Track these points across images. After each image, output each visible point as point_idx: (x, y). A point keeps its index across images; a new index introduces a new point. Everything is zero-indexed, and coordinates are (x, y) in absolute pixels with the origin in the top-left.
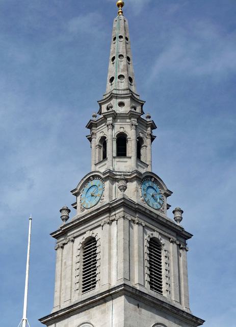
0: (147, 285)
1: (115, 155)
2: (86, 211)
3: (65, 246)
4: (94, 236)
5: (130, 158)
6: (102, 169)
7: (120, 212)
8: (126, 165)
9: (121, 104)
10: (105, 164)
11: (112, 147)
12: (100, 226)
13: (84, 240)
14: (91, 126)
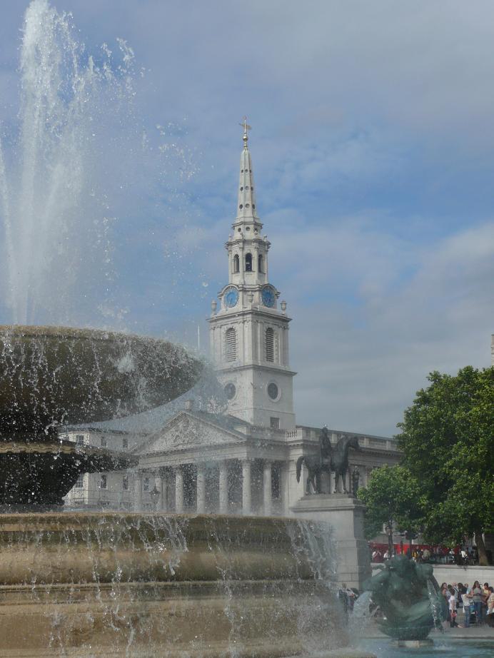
7: (249, 317)
8: (252, 279)
9: (248, 229)
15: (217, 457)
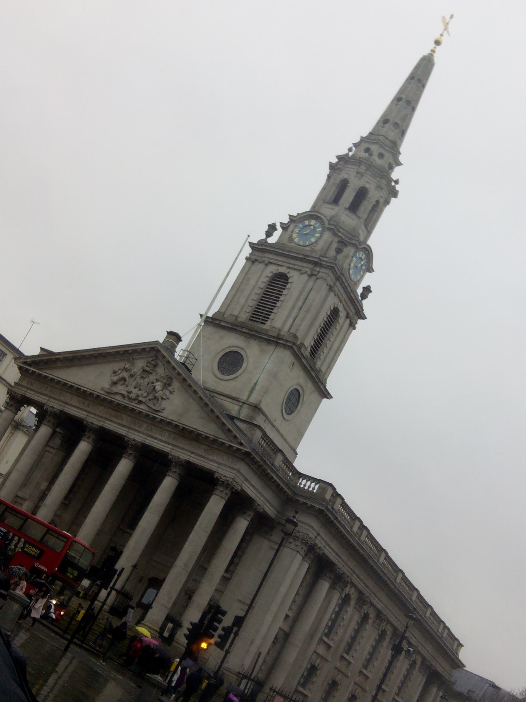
0: (309, 349)
1: (347, 207)
2: (293, 245)
3: (256, 263)
4: (289, 276)
5: (359, 217)
6: (328, 211)
9: (381, 156)
10: (333, 209)
11: (348, 196)
12: (300, 270)
13: (277, 272)
14: (341, 158)
15: (182, 452)
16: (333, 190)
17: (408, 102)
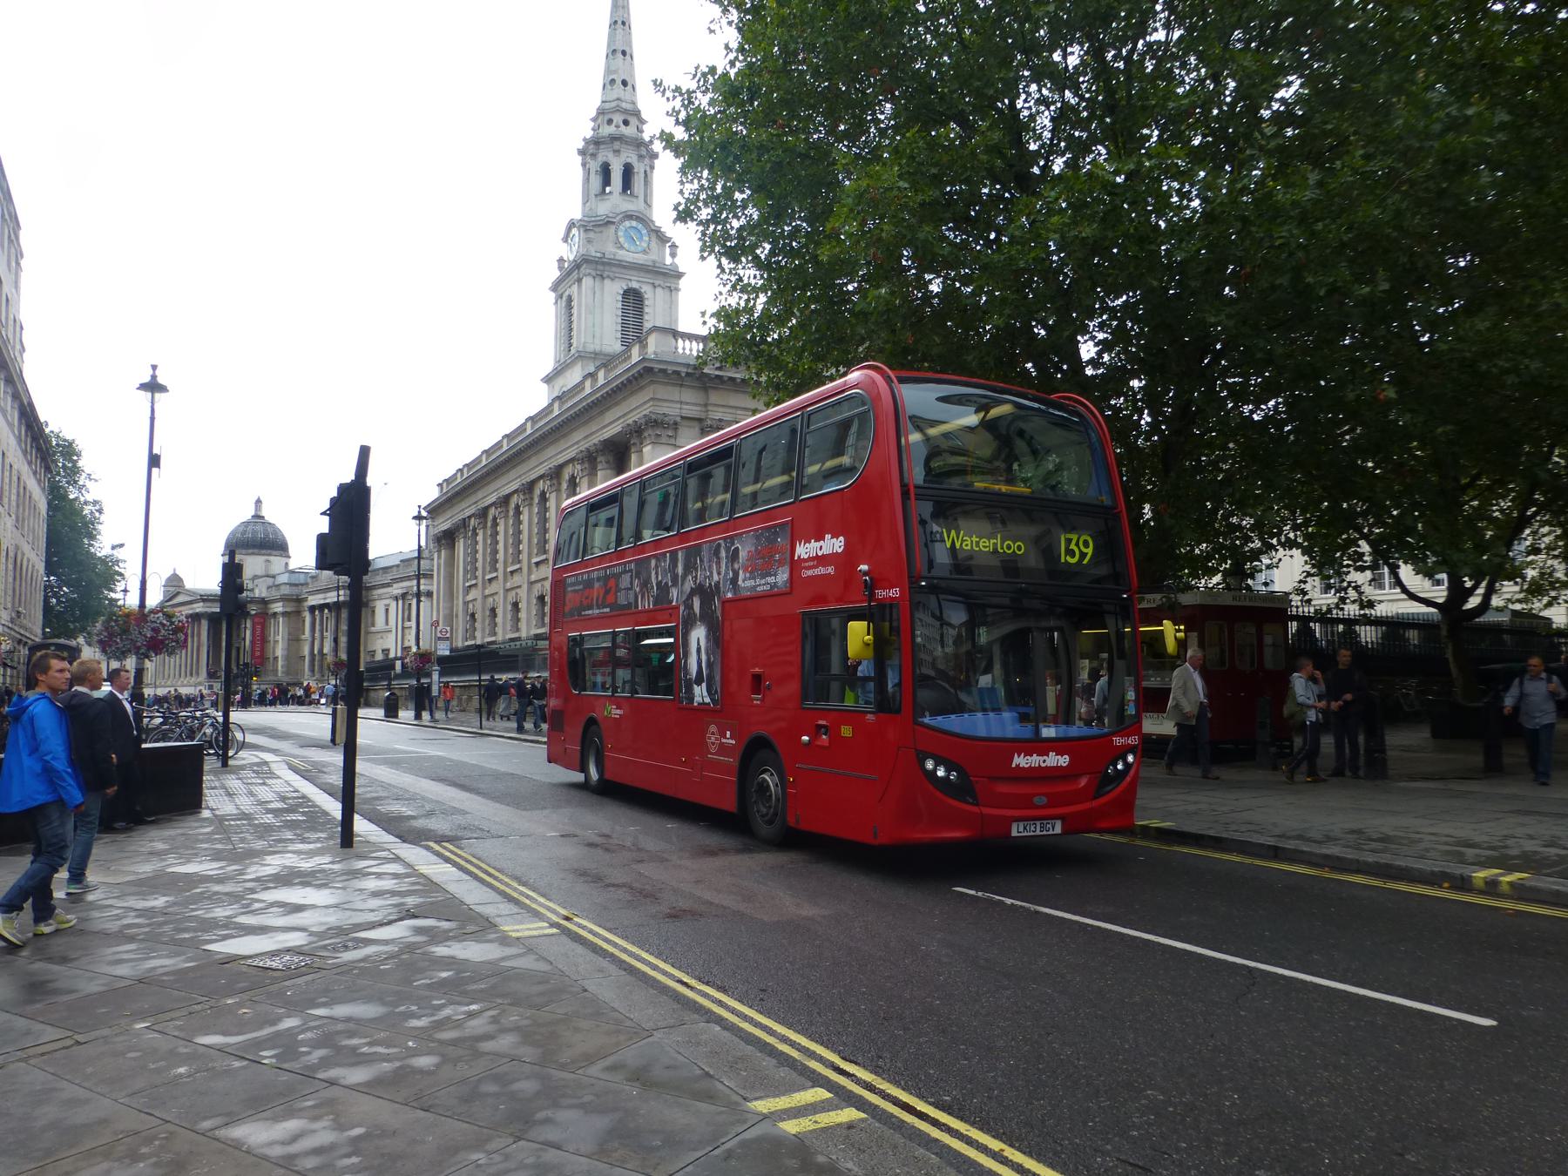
9: (626, 123)
16: (596, 181)
17: (624, 53)
